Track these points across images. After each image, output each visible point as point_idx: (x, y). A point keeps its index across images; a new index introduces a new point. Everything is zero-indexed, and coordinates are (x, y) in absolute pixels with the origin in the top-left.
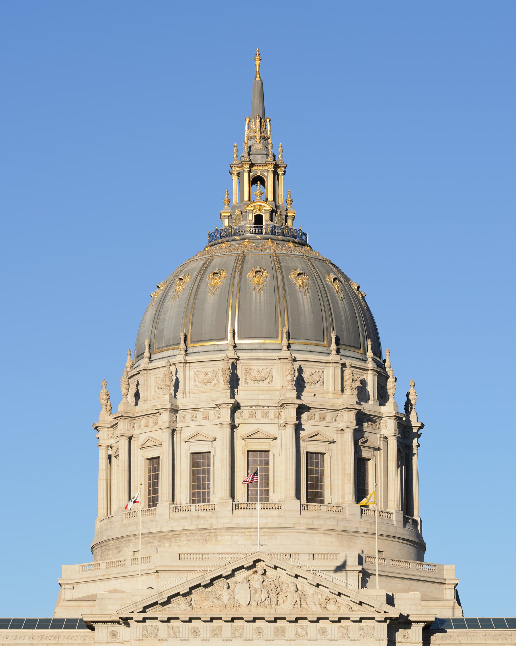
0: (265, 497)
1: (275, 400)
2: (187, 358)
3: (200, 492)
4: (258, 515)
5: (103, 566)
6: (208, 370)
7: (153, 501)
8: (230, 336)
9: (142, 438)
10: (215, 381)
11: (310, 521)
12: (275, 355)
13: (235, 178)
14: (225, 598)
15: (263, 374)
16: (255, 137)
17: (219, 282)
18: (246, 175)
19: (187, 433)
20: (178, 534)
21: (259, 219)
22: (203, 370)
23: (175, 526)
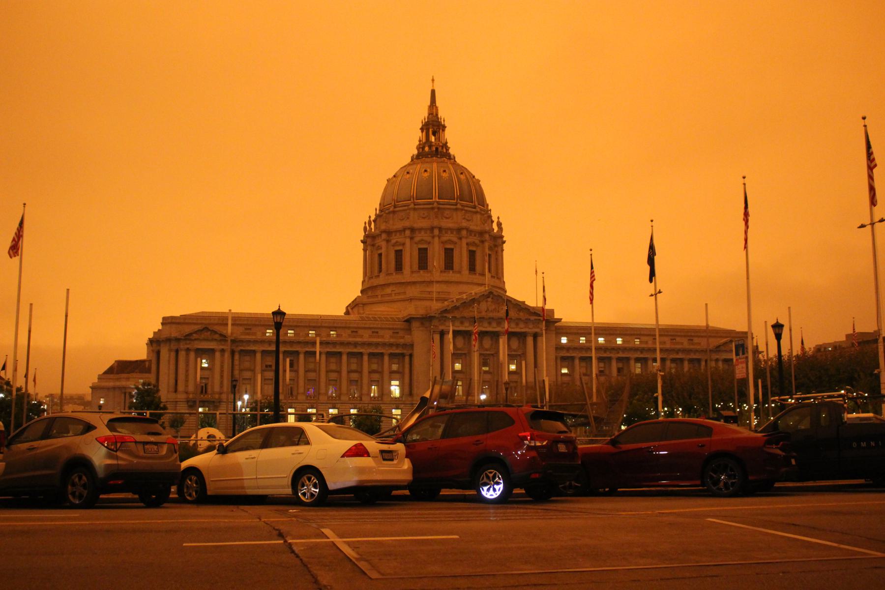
0: (452, 269)
1: (456, 226)
17: (426, 175)
19: (417, 239)
20: (414, 283)
23: (413, 280)
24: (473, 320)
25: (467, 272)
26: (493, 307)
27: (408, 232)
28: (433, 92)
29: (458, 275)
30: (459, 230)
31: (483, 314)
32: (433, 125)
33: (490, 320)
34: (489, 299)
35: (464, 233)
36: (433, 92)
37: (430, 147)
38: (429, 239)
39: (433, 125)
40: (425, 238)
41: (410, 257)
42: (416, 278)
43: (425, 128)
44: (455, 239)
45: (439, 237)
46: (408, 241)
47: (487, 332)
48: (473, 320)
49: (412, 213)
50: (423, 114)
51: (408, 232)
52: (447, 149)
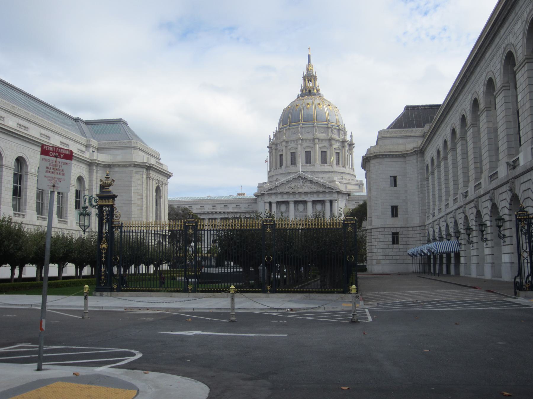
3: (293, 162)
12: (312, 125)
21: (310, 91)
27: (284, 144)
28: (309, 56)
30: (314, 139)
32: (309, 77)
35: (316, 141)
36: (309, 56)
37: (306, 90)
39: (309, 77)
41: (287, 159)
43: (304, 78)
44: (312, 145)
45: (301, 145)
46: (284, 149)
47: (301, 201)
50: (303, 71)
52: (318, 90)
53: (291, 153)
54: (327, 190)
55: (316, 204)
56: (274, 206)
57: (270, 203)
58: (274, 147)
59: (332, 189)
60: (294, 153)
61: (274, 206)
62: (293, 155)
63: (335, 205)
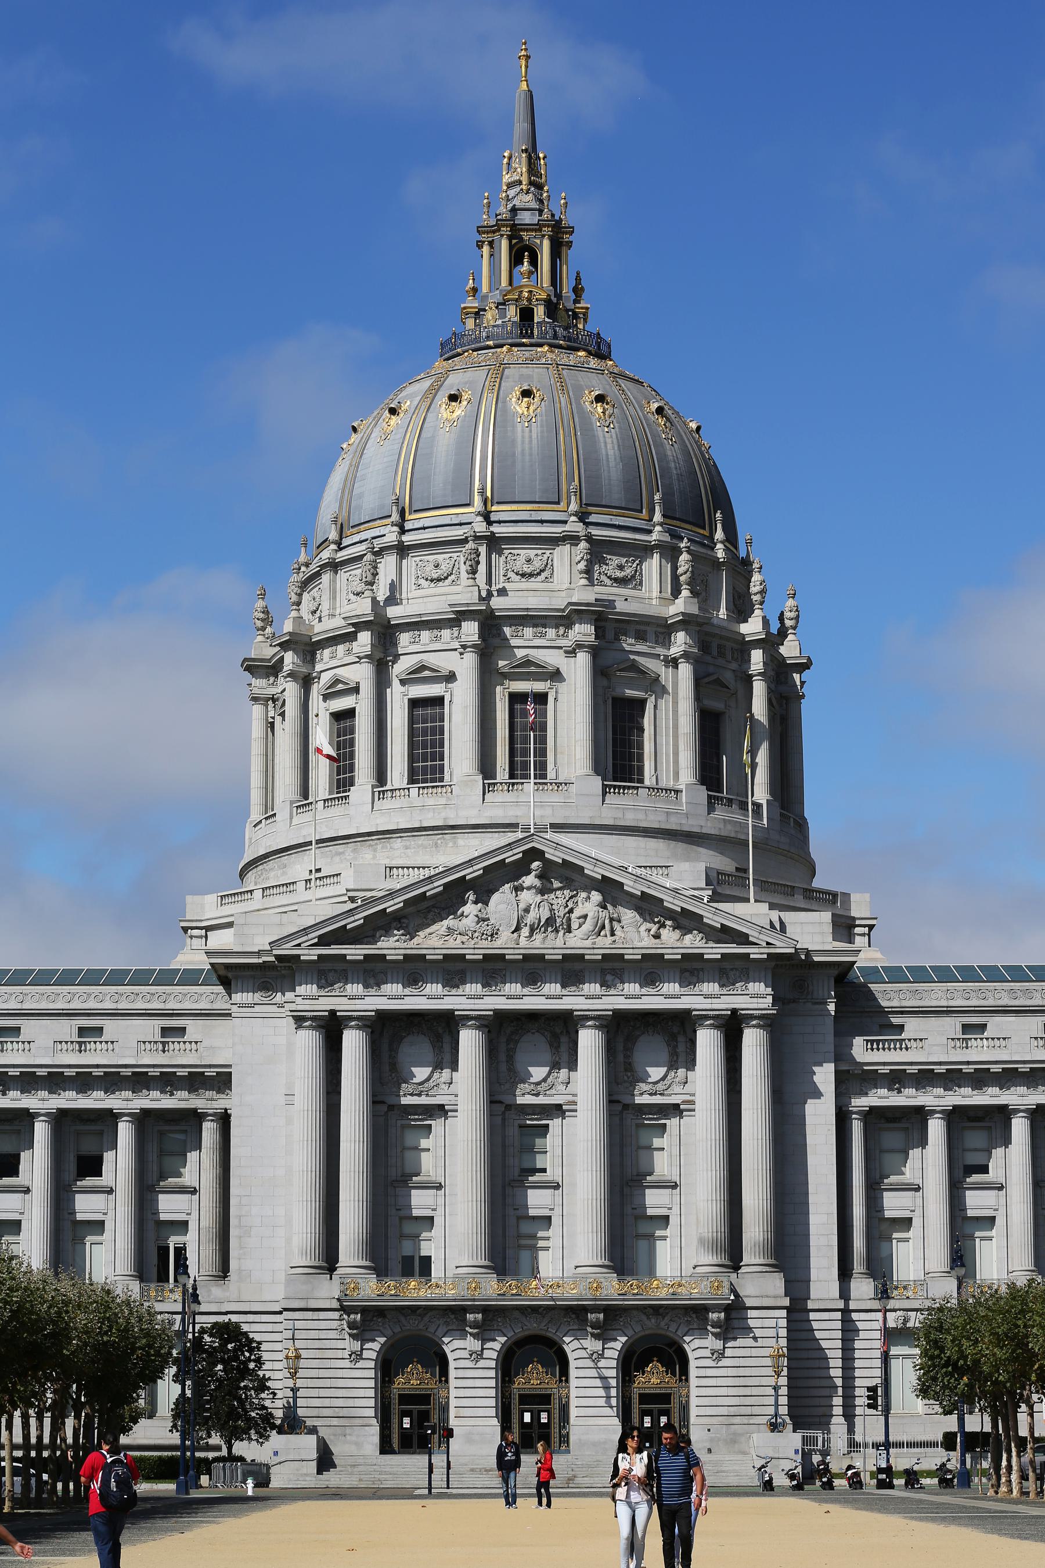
1: (559, 602)
2: (405, 538)
3: (427, 765)
4: (526, 805)
5: (258, 894)
6: (440, 557)
7: (343, 782)
8: (477, 500)
9: (326, 678)
10: (453, 577)
11: (620, 815)
13: (486, 249)
14: (469, 922)
15: (537, 564)
16: (520, 183)
17: (459, 410)
18: (504, 243)
21: (526, 314)
22: (431, 558)
24: (453, 970)
25: (597, 782)
26: (545, 914)
29: (553, 797)
30: (565, 619)
31: (506, 943)
33: (532, 969)
34: (529, 880)
38: (444, 662)
40: (432, 660)
42: (394, 813)
44: (553, 659)
46: (362, 674)
48: (453, 970)
49: (388, 565)
51: (365, 638)
53: (415, 704)
54: (714, 951)
55: (630, 1042)
56: (353, 1044)
57: (331, 1029)
58: (290, 659)
59: (743, 939)
60: (439, 701)
61: (353, 1044)
62: (426, 712)
63: (753, 1043)
